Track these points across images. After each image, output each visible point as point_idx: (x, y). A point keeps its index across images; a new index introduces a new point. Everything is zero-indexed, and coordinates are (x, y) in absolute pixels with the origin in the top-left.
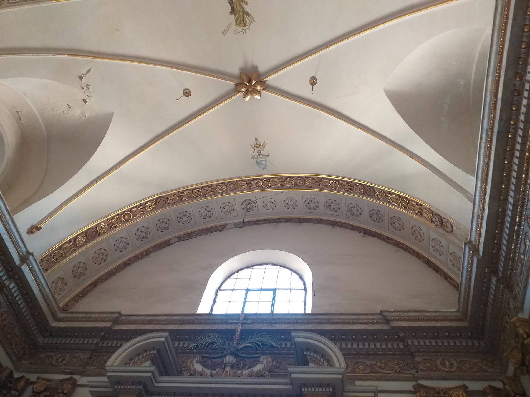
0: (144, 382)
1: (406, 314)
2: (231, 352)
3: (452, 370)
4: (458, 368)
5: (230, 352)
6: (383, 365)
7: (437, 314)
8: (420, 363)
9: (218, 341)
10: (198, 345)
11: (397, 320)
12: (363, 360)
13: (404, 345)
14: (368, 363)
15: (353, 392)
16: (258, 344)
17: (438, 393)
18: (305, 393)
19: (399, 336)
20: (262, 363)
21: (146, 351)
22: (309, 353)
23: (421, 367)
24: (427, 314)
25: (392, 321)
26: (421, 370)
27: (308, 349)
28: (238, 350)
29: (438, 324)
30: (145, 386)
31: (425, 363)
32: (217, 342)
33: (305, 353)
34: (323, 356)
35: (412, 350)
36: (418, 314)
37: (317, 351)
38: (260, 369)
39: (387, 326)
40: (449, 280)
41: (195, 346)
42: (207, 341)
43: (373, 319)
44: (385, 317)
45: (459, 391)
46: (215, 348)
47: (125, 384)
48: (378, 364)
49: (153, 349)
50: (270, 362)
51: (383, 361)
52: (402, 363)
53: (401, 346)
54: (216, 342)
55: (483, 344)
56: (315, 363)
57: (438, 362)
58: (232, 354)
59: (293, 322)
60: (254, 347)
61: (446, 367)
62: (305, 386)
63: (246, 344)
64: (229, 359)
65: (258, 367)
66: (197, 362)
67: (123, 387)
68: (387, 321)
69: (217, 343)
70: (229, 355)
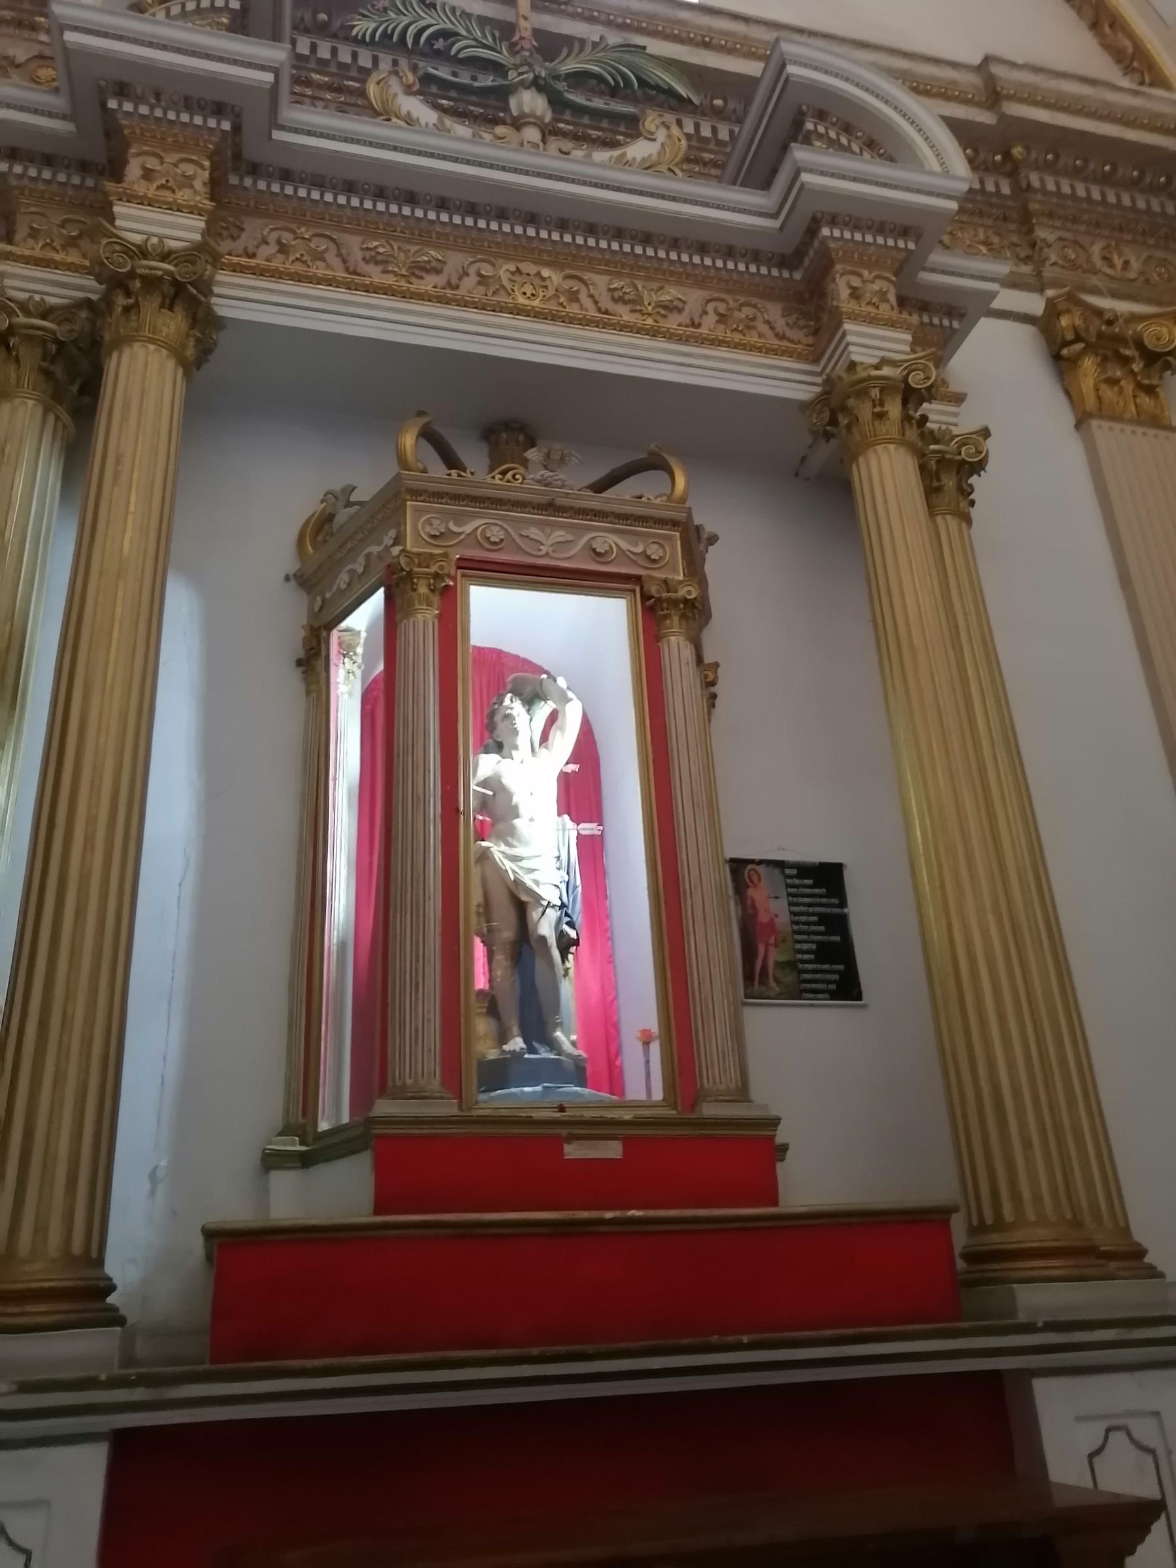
0: (237, 110)
2: (536, 77)
4: (1142, 273)
5: (531, 76)
8: (1049, 246)
9: (468, 30)
10: (387, 28)
11: (1022, 101)
15: (944, 272)
16: (623, 76)
17: (1110, 323)
18: (832, 245)
19: (1007, 155)
22: (821, 129)
23: (1053, 258)
25: (1011, 98)
26: (1054, 264)
28: (557, 77)
29: (1131, 135)
30: (237, 129)
31: (1064, 247)
32: (464, 33)
33: (809, 126)
36: (1085, 90)
38: (650, 156)
40: (1107, 30)
41: (375, 30)
42: (422, 23)
43: (954, 83)
45: (1161, 325)
46: (461, 56)
47: (153, 101)
50: (680, 140)
53: (1006, 190)
54: (458, 34)
57: (1096, 249)
58: (537, 84)
59: (699, 38)
60: (612, 83)
61: (1112, 265)
62: (833, 221)
63: (579, 63)
64: (530, 102)
65: (639, 150)
67: (144, 110)
68: (993, 96)
69: (467, 38)
70: (528, 88)
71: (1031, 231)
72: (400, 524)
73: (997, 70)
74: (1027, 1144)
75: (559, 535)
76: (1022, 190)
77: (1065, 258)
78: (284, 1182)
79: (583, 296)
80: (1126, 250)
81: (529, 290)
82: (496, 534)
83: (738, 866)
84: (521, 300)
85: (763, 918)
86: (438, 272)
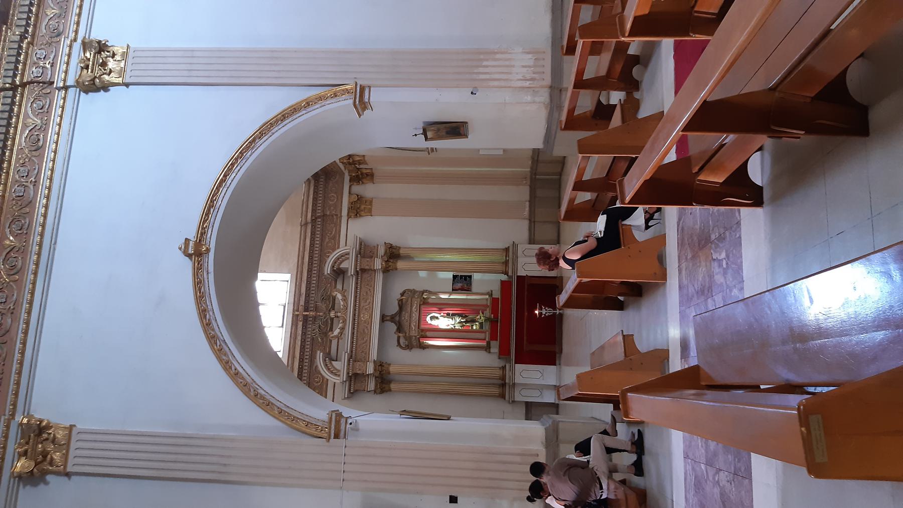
1: (304, 212)
3: (335, 196)
6: (330, 233)
7: (305, 194)
8: (331, 212)
12: (325, 243)
13: (319, 218)
14: (327, 240)
20: (336, 294)
21: (326, 365)
24: (305, 200)
25: (306, 221)
27: (333, 267)
34: (338, 259)
35: (322, 214)
37: (335, 262)
39: (309, 224)
44: (304, 225)
48: (328, 235)
49: (325, 360)
51: (327, 232)
52: (328, 222)
53: (320, 220)
55: (322, 177)
56: (341, 263)
57: (331, 203)
61: (334, 200)
66: (333, 333)
68: (306, 224)
71: (326, 215)
72: (412, 336)
73: (303, 223)
74: (494, 268)
75: (414, 315)
76: (319, 217)
77: (333, 210)
78: (492, 350)
79: (366, 307)
80: (330, 195)
81: (366, 316)
82: (414, 324)
83: (453, 290)
84: (368, 317)
85: (460, 287)
86: (364, 330)
